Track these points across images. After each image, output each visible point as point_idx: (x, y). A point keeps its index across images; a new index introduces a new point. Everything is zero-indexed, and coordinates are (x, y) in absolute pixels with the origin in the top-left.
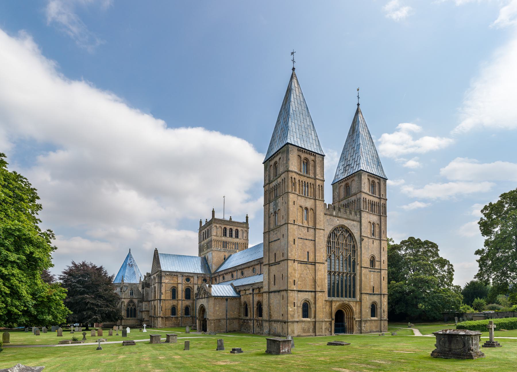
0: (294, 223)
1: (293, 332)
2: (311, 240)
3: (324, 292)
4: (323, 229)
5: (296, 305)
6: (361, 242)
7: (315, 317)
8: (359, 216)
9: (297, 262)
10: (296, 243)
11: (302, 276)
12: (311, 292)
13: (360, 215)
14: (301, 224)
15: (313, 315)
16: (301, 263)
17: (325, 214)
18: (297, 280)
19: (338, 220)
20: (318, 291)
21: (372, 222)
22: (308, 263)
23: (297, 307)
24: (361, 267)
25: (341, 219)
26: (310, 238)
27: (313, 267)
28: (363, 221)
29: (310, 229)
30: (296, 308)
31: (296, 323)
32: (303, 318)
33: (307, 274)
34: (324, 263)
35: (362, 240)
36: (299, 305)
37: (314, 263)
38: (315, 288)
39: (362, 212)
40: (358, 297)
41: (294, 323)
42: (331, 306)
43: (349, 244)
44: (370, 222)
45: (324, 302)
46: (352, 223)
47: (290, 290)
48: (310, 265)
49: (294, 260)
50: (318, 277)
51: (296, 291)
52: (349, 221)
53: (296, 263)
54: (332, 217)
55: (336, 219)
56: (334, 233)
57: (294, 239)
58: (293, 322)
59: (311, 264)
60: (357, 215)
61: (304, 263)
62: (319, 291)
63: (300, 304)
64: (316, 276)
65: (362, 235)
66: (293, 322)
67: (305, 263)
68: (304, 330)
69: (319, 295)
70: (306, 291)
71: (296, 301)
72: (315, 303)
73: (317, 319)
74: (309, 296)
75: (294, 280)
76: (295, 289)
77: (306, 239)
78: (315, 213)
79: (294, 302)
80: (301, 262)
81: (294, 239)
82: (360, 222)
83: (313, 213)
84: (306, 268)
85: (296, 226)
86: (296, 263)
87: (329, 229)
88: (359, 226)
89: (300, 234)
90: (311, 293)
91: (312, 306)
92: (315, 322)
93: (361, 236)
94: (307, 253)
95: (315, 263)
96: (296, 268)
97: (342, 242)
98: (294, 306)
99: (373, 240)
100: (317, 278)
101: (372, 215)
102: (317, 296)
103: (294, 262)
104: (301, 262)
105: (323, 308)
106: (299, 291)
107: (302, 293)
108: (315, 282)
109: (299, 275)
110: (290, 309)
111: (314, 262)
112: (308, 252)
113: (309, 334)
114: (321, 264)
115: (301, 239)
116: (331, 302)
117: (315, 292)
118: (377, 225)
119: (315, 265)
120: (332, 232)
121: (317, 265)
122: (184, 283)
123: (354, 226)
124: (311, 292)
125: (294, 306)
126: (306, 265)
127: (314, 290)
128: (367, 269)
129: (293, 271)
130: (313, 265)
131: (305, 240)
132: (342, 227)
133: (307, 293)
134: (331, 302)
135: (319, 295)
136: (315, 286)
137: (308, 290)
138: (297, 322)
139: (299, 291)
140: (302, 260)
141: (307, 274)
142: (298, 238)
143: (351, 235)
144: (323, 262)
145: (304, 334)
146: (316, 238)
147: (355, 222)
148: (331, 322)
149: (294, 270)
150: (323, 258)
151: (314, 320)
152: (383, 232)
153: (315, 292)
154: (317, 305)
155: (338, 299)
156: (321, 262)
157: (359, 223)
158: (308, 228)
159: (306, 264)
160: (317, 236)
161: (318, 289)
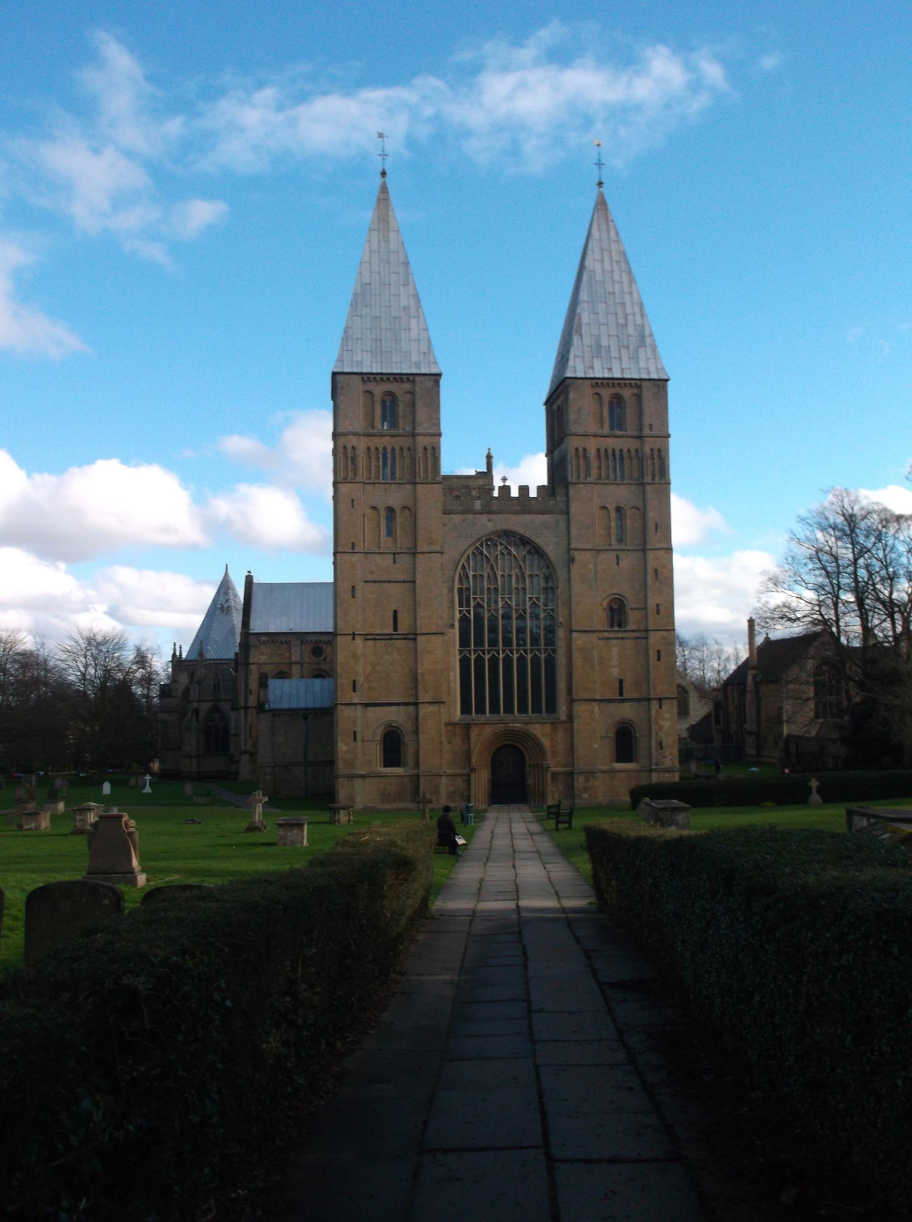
0: (353, 549)
1: (352, 799)
2: (404, 582)
3: (443, 703)
4: (439, 549)
5: (359, 736)
6: (569, 567)
7: (417, 765)
8: (565, 498)
9: (363, 637)
10: (359, 593)
11: (378, 668)
12: (406, 704)
13: (567, 495)
14: (374, 548)
15: (410, 760)
16: (375, 639)
17: (447, 512)
18: (361, 680)
19: (490, 520)
20: (424, 703)
21: (612, 507)
22: (395, 637)
23: (363, 741)
24: (572, 631)
25: (500, 516)
26: (401, 577)
27: (411, 644)
28: (572, 510)
29: (401, 555)
30: (359, 743)
31: (359, 780)
32: (385, 766)
33: (391, 664)
34: (442, 634)
35: (571, 560)
36: (368, 736)
37: (412, 636)
38: (416, 695)
39: (570, 485)
40: (562, 714)
41: (355, 779)
43: (489, 589)
44: (604, 508)
45: (443, 727)
46: (540, 517)
47: (341, 704)
48: (403, 641)
49: (354, 634)
50: (424, 668)
51: (359, 707)
52: (528, 517)
53: (359, 641)
54: (470, 517)
55: (484, 518)
56: (481, 553)
57: (353, 587)
58: (351, 777)
59: (405, 639)
60: (555, 497)
61: (382, 637)
62: (428, 703)
64: (419, 665)
65: (572, 546)
66: (351, 777)
67: (388, 638)
68: (385, 796)
69: (429, 710)
70: (390, 704)
71: (358, 729)
72: (416, 732)
73: (423, 769)
75: (354, 681)
76: (356, 701)
77: (389, 582)
78: (415, 517)
79: (355, 732)
80: (376, 637)
81: (353, 587)
82: (568, 513)
83: (411, 516)
84: (390, 649)
85: (357, 556)
86: (359, 641)
88: (563, 526)
89: (372, 573)
90: (404, 707)
91: (408, 738)
92: (418, 776)
93: (569, 549)
94: (391, 615)
95: (415, 634)
96: (359, 652)
97: (507, 572)
98: (355, 741)
99: (618, 553)
100: (419, 671)
101: (611, 487)
102: (421, 714)
103: (354, 639)
104: (376, 637)
105: (441, 743)
106: (367, 705)
107: (378, 709)
108: (415, 679)
109: (369, 668)
110: (342, 747)
111: (413, 632)
112: (395, 613)
113: (401, 805)
114: (433, 637)
115: (374, 582)
116: (467, 727)
117: (416, 704)
118: (629, 513)
119: (415, 639)
120: (474, 553)
121: (420, 638)
122: (307, 660)
123: (547, 528)
124: (406, 704)
125: (355, 741)
126: (391, 642)
127: (411, 700)
128: (591, 635)
129: (352, 661)
130: (411, 641)
131: (387, 584)
132: (507, 534)
133: (393, 708)
134: (467, 727)
135: (429, 710)
136: (416, 688)
137: (395, 700)
138: (363, 777)
139: (367, 705)
140: (379, 632)
141: (391, 664)
142: (366, 582)
143: (537, 551)
144: (439, 630)
145: (388, 806)
146: (418, 576)
147: (547, 517)
148: (469, 775)
149: (354, 656)
150: (440, 622)
151: (415, 772)
152: (653, 527)
153: (416, 704)
154: (422, 736)
155: (481, 718)
156: (434, 631)
157: (565, 517)
158: (394, 554)
159: (390, 639)
160: (419, 569)
161: (423, 697)
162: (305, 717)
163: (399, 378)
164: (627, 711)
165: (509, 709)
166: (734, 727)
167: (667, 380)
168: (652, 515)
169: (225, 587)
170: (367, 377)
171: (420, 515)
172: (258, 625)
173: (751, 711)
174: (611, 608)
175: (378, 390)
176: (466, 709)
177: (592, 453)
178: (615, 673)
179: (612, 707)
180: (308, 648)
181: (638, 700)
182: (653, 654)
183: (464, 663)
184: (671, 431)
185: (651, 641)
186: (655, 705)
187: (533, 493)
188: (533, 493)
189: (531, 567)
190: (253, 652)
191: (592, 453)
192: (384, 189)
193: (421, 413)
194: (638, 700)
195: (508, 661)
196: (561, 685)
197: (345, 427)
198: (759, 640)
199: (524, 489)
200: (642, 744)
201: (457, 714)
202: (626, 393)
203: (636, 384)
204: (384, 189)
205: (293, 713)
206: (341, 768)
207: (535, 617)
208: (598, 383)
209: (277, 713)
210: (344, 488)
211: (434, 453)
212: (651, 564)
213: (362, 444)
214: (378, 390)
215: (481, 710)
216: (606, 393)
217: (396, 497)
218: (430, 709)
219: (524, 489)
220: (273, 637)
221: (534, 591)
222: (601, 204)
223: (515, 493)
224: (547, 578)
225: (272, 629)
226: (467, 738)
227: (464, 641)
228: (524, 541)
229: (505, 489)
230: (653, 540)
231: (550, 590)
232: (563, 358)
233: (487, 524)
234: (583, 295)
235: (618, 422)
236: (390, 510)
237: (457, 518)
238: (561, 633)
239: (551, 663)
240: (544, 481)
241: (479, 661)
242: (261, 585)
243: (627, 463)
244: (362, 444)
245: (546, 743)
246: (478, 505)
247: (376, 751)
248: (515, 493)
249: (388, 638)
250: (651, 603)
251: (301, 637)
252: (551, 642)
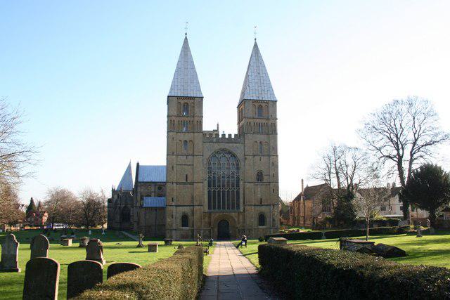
5: (174, 217)
7: (193, 226)
10: (175, 169)
15: (190, 223)
18: (175, 198)
40: (242, 208)
42: (210, 217)
52: (231, 144)
63: (179, 216)
67: (184, 183)
74: (187, 210)
80: (180, 183)
87: (208, 154)
88: (242, 148)
104: (180, 183)
108: (193, 198)
143: (234, 156)
149: (173, 190)
162: (156, 210)
163: (190, 98)
164: (263, 209)
165: (224, 208)
166: (296, 215)
167: (276, 101)
168: (272, 144)
169: (129, 167)
170: (179, 98)
171: (196, 144)
172: (140, 179)
173: (302, 210)
174: (258, 175)
175: (182, 102)
176: (209, 208)
177: (252, 124)
178: (259, 196)
179: (258, 208)
180: (157, 187)
181: (267, 205)
182: (272, 190)
183: (209, 192)
184: (278, 117)
185: (271, 186)
186: (272, 207)
187: (233, 137)
188: (233, 137)
189: (232, 161)
190: (139, 188)
191: (252, 124)
192: (186, 38)
193: (197, 110)
194: (267, 205)
195: (224, 192)
196: (241, 200)
197: (172, 113)
198: (304, 187)
199: (230, 135)
200: (268, 220)
201: (206, 209)
202: (264, 105)
203: (267, 102)
204: (186, 38)
205: (151, 208)
206: (167, 227)
207: (233, 177)
208: (254, 101)
209: (147, 208)
210: (171, 134)
211: (200, 123)
212: (271, 161)
213: (176, 120)
214: (182, 102)
215: (214, 208)
216: (257, 105)
217: (188, 137)
218: (198, 207)
219: (230, 135)
220: (145, 183)
221: (233, 169)
222: (256, 45)
223: (227, 136)
224: (237, 165)
225: (145, 181)
226: (210, 217)
227: (209, 186)
228: (230, 153)
229: (224, 135)
230: (272, 153)
231: (238, 169)
232: (243, 93)
233: (217, 147)
234: (250, 74)
235: (260, 115)
236: (186, 141)
237: (207, 145)
238: (241, 183)
239: (238, 193)
240: (236, 133)
241: (214, 191)
242: (142, 166)
243: (263, 128)
244: (176, 120)
245: (236, 219)
246: (215, 140)
247: (179, 221)
248: (227, 136)
249: (184, 183)
250: (271, 174)
251: (155, 183)
252: (238, 185)
